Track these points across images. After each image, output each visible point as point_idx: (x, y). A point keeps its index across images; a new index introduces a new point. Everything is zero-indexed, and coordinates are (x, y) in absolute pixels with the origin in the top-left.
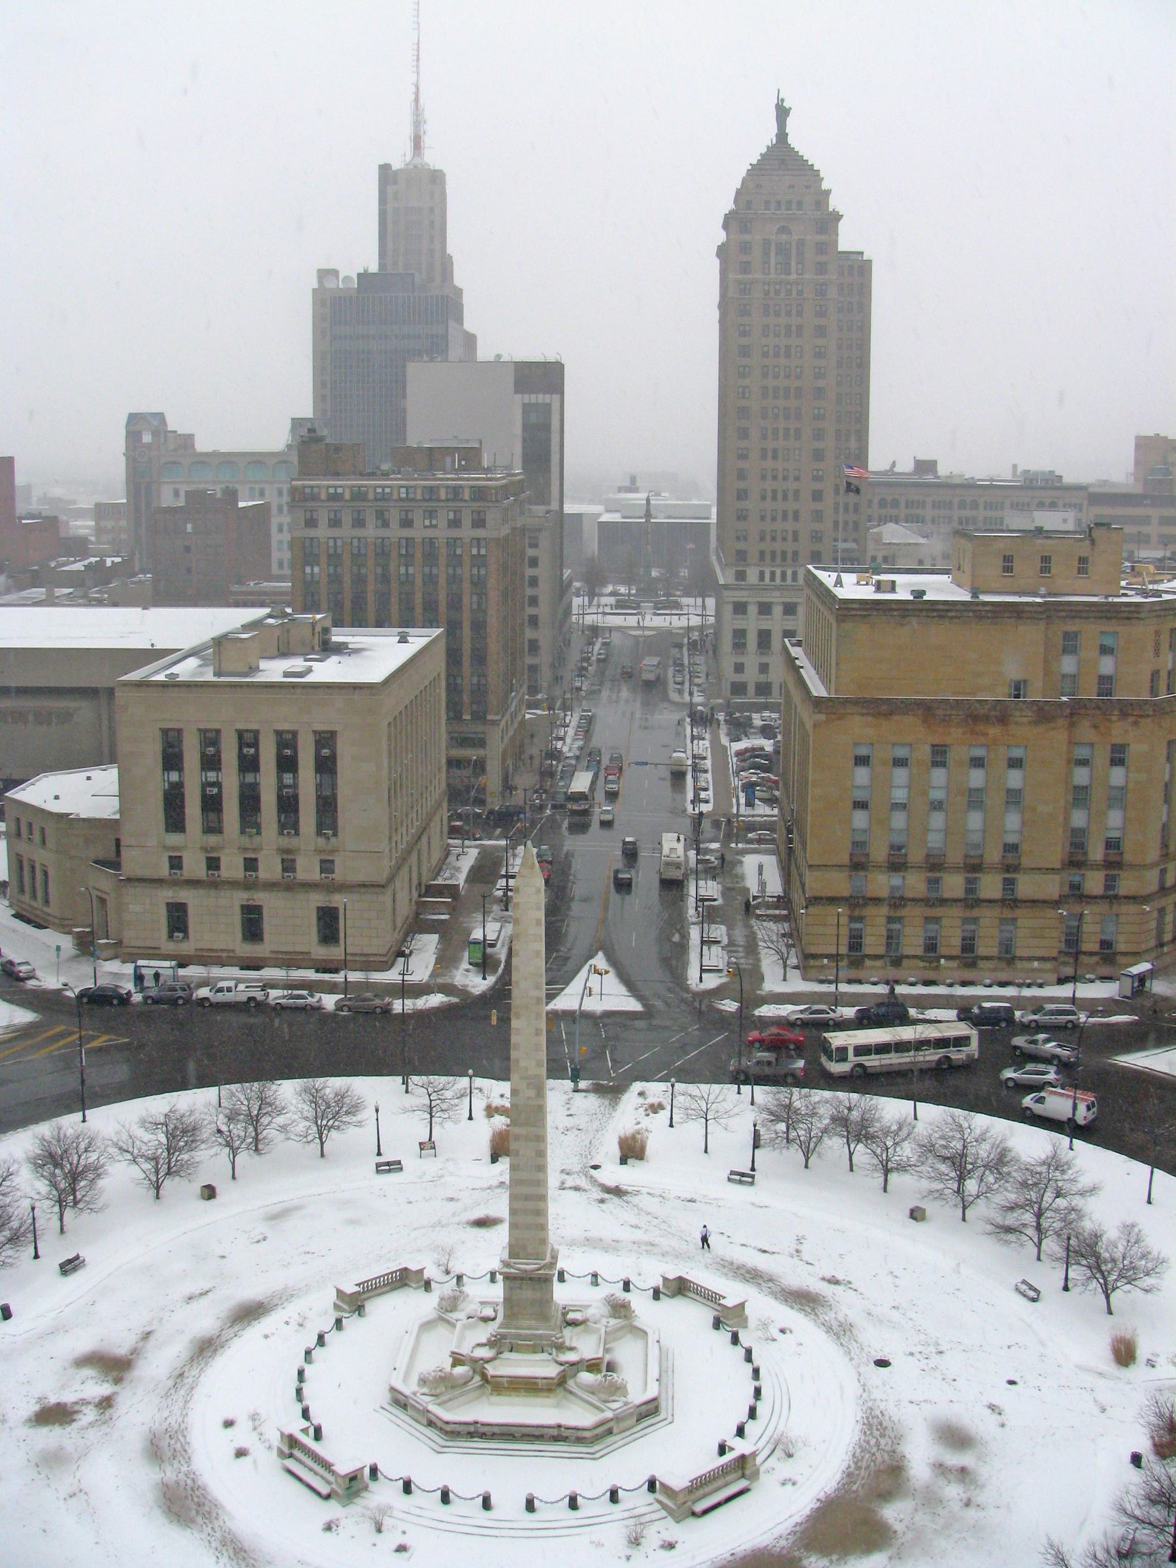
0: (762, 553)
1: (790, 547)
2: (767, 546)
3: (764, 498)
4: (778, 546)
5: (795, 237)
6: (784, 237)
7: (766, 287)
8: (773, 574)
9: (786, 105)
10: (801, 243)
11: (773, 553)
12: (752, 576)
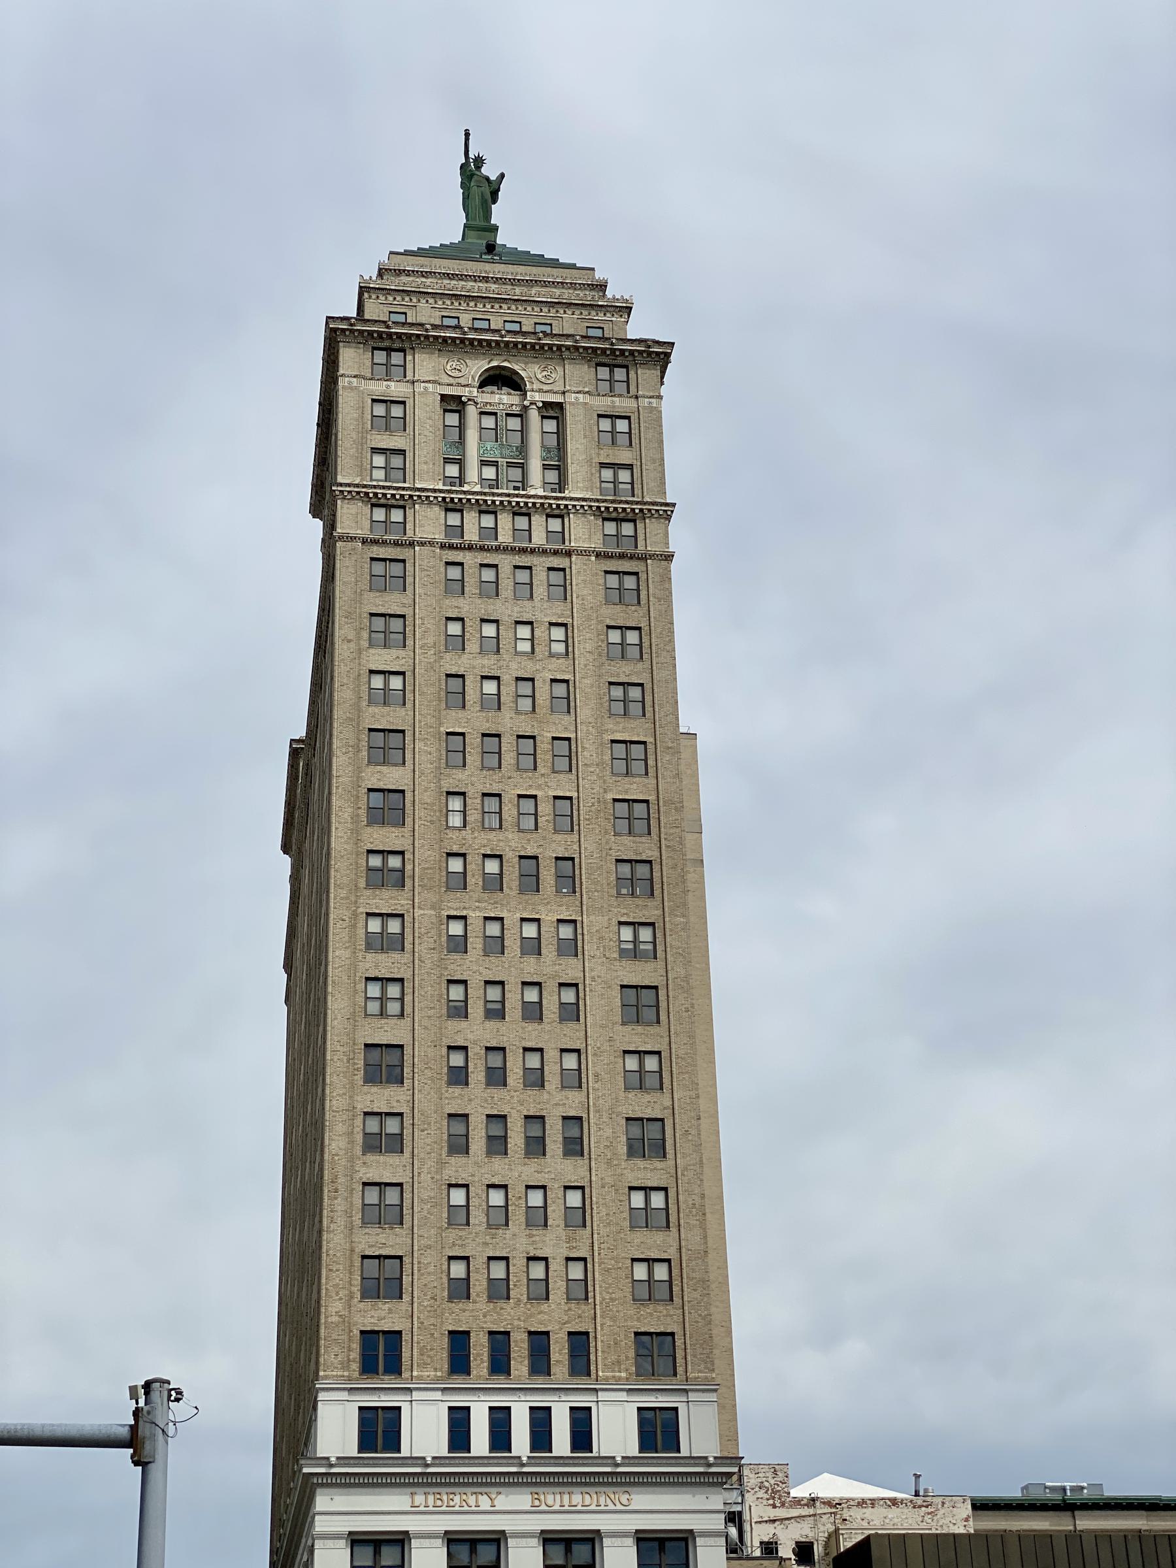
0: (459, 1341)
1: (557, 1318)
2: (479, 1317)
3: (459, 1146)
4: (517, 1318)
5: (537, 397)
6: (504, 399)
7: (454, 519)
8: (500, 1420)
9: (490, 171)
10: (554, 411)
11: (500, 1341)
12: (424, 1431)
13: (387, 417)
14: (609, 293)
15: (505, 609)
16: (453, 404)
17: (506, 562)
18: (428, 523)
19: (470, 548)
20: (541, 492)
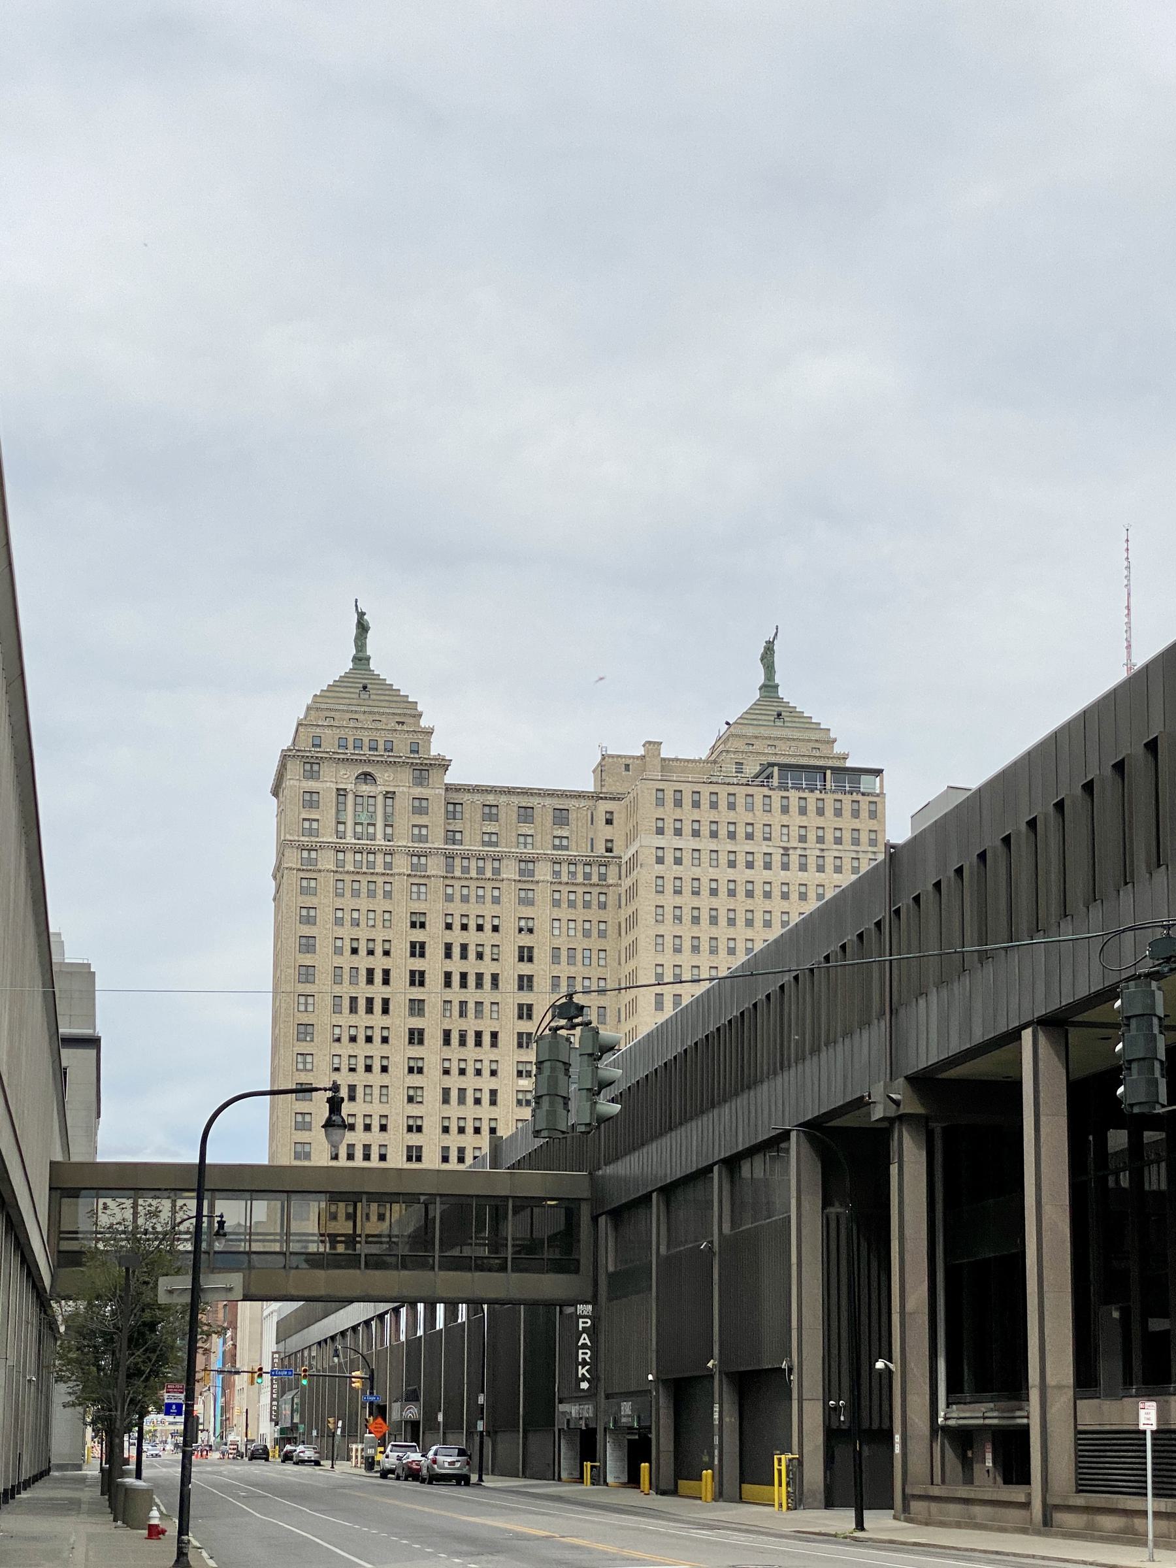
6: (365, 789)
13: (311, 801)
14: (424, 723)
15: (364, 903)
16: (341, 793)
17: (364, 880)
18: (327, 861)
19: (347, 872)
20: (382, 842)
